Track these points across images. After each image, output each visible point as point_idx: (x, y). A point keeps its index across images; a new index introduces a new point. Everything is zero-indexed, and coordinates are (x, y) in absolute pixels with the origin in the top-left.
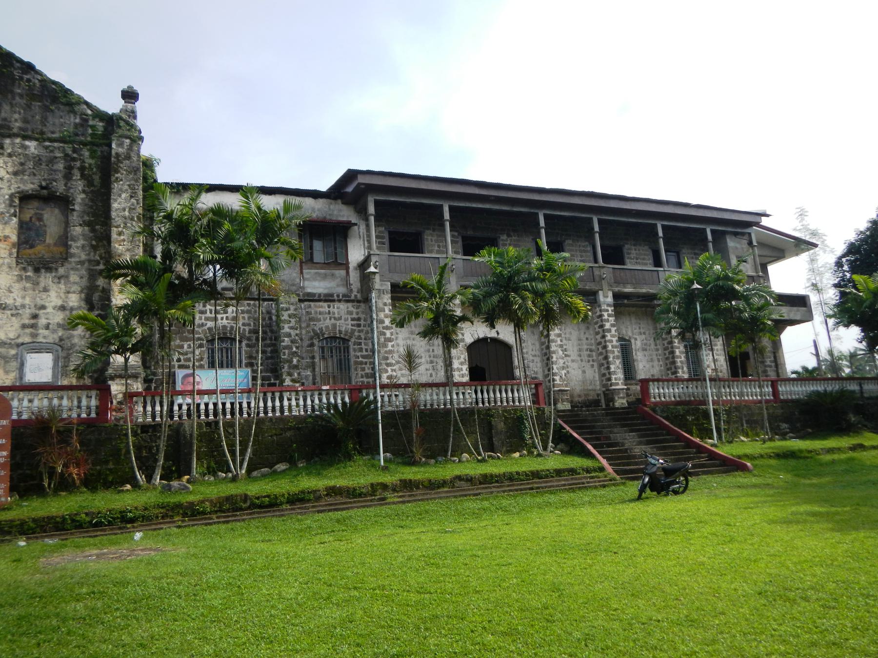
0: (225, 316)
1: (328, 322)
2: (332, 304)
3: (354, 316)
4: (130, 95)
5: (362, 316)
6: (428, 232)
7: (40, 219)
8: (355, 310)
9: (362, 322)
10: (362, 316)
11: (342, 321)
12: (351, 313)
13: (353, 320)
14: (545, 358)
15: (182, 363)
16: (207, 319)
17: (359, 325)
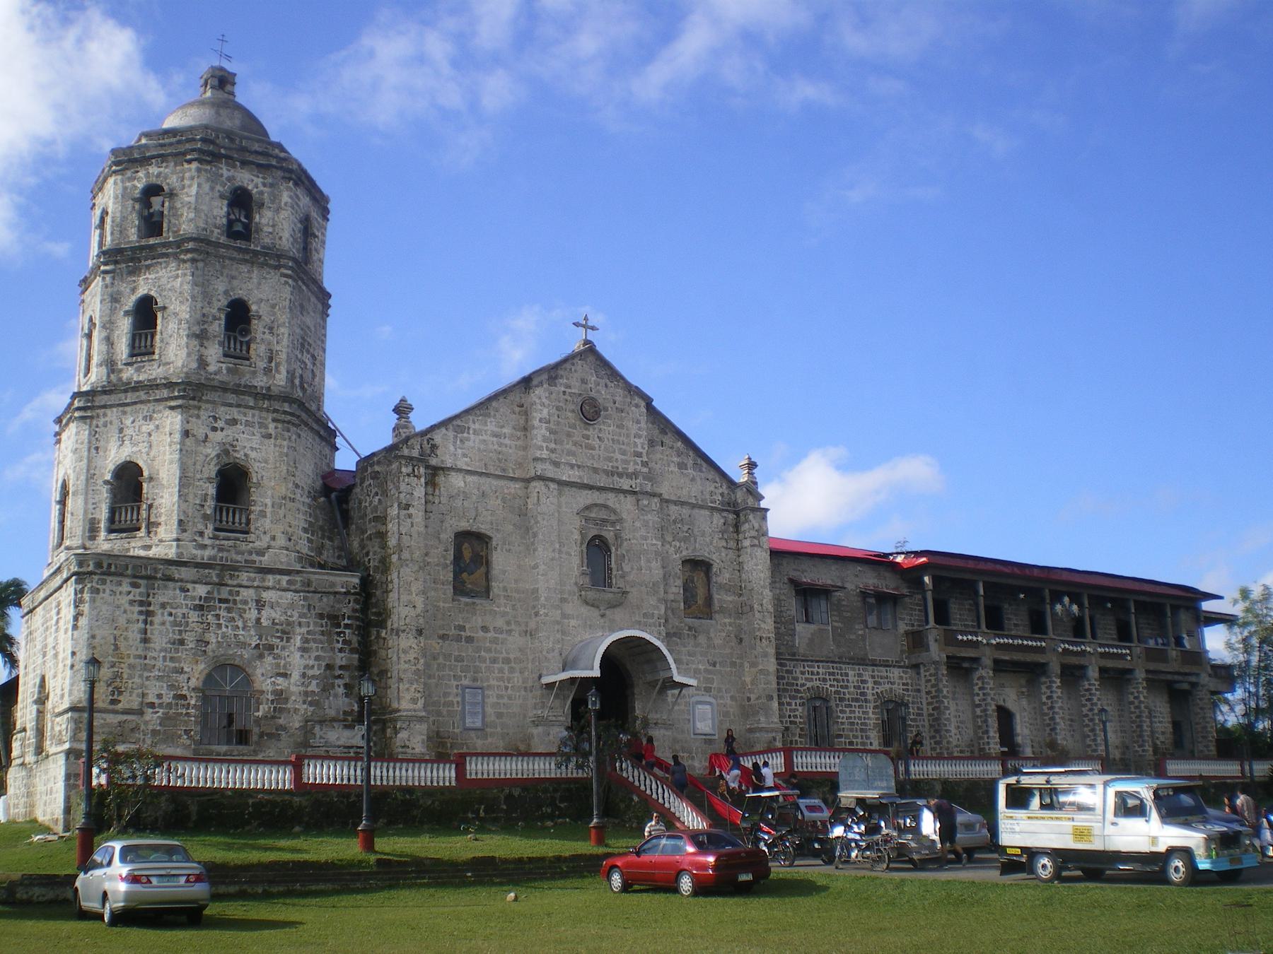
0: (817, 677)
1: (887, 686)
2: (888, 669)
3: (905, 681)
4: (752, 465)
5: (909, 681)
6: (953, 600)
7: (692, 582)
8: (904, 676)
9: (910, 687)
10: (909, 681)
11: (896, 686)
12: (901, 678)
13: (903, 684)
14: (1048, 729)
15: (792, 719)
16: (807, 679)
17: (908, 690)
